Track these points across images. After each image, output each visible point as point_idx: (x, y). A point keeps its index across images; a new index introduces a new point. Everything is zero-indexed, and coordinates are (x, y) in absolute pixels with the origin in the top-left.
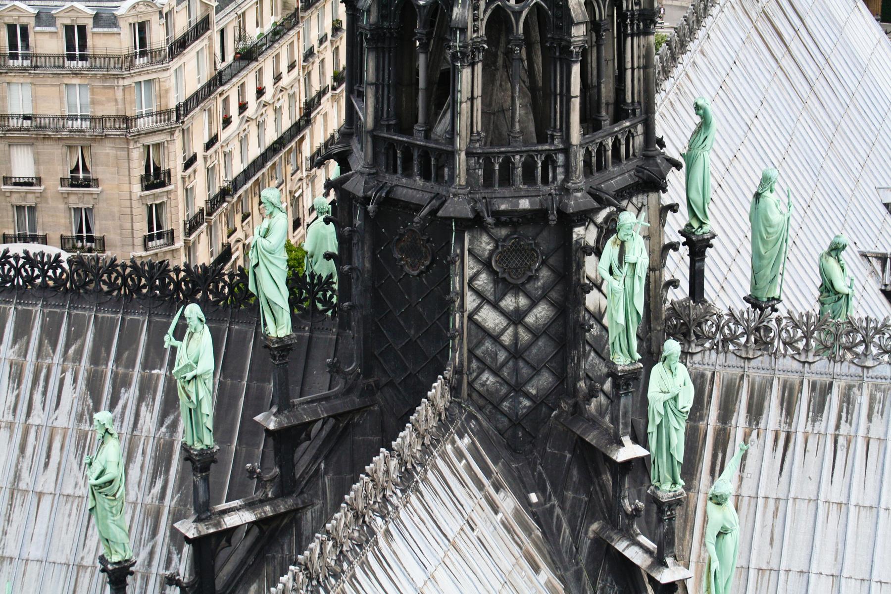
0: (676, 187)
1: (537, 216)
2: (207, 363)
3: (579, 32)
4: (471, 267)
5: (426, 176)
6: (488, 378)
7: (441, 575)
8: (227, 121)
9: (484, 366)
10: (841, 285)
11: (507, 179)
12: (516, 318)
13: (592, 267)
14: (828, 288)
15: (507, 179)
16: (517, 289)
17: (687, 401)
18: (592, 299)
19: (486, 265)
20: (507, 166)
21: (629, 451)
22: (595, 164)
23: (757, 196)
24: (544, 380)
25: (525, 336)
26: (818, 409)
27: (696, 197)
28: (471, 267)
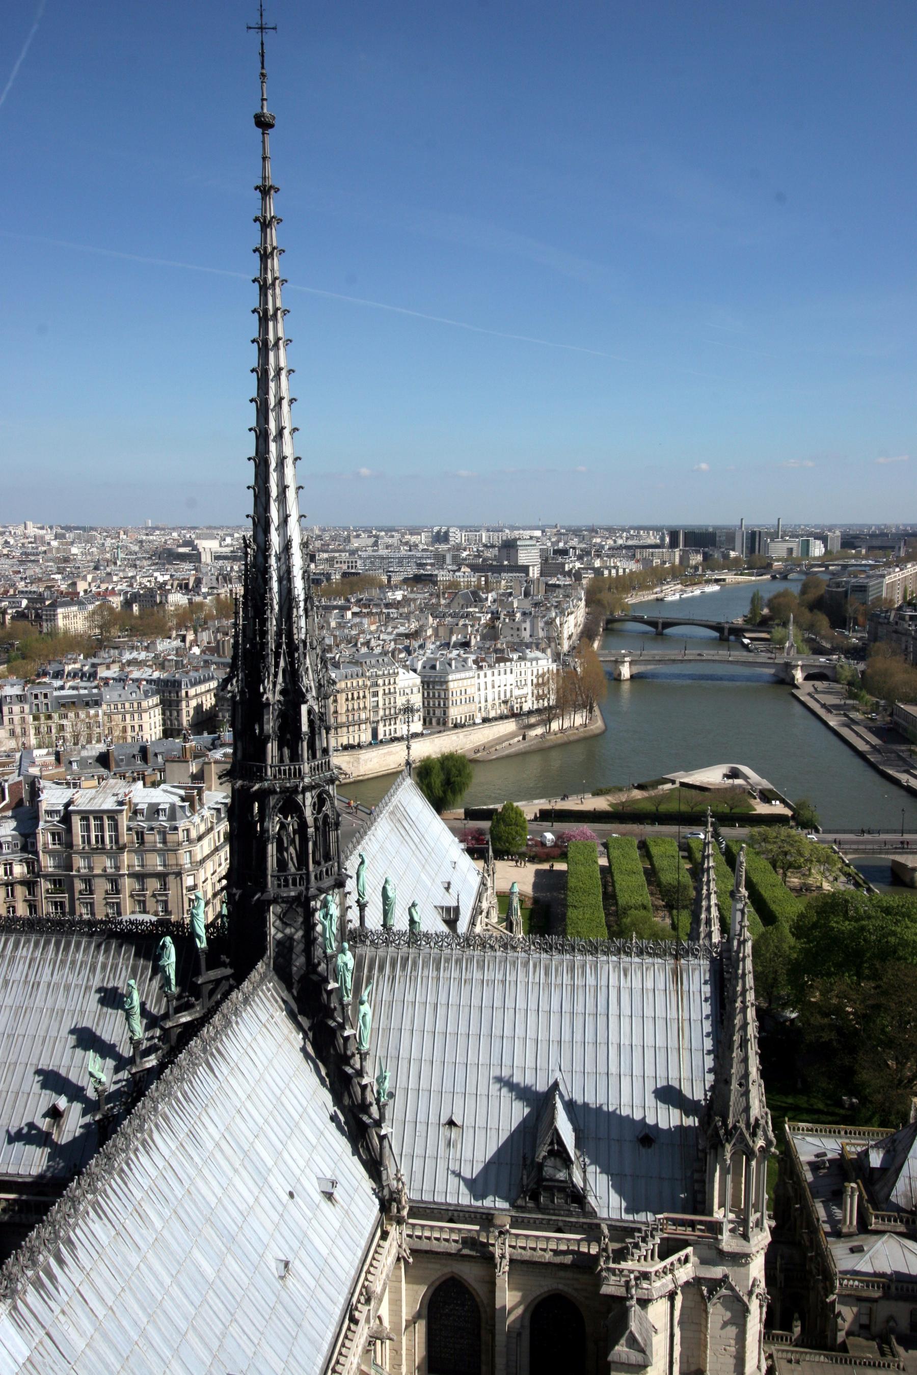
0: (350, 885)
1: (297, 898)
2: (173, 958)
3: (311, 830)
7: (259, 1037)
8: (220, 865)
10: (416, 918)
11: (286, 885)
13: (319, 915)
14: (412, 922)
15: (286, 885)
16: (290, 925)
17: (351, 964)
18: (319, 928)
20: (286, 880)
21: (332, 985)
22: (319, 878)
23: (384, 888)
26: (404, 967)
27: (361, 888)
28: (272, 918)
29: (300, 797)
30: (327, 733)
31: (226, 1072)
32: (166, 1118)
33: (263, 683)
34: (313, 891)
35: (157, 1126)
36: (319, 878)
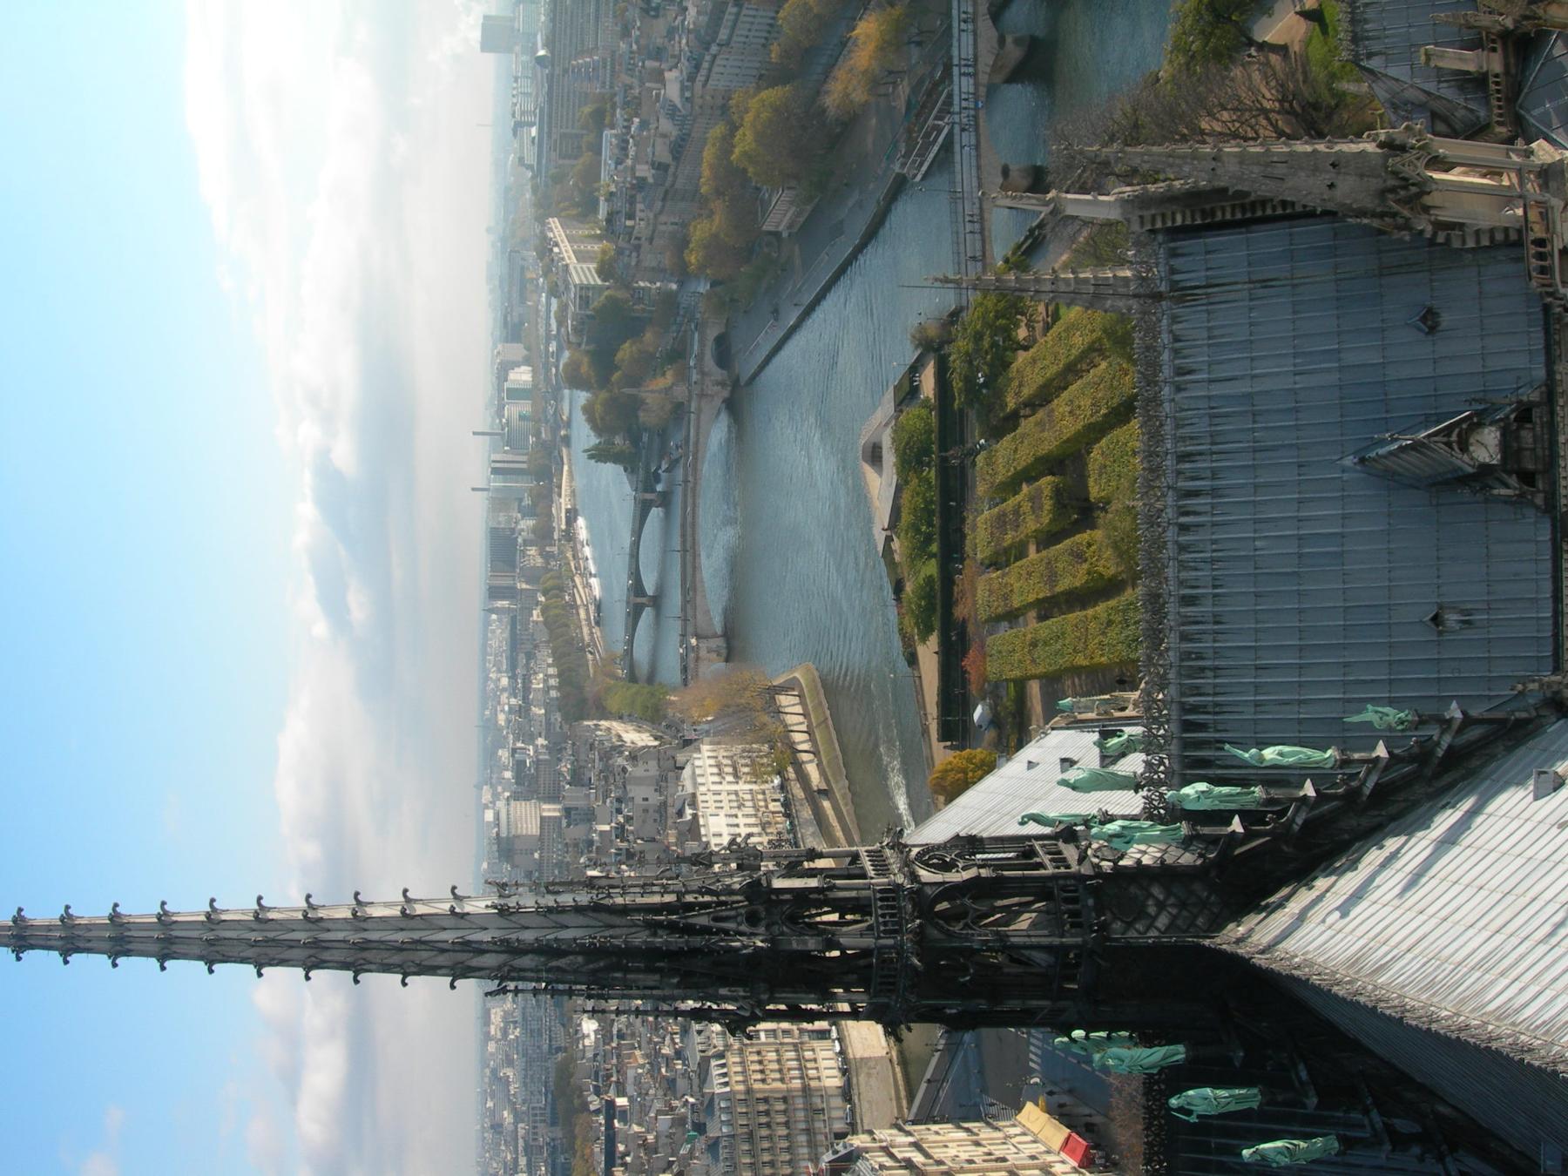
2: (1208, 1091)
3: (984, 873)
4: (1132, 934)
5: (1077, 965)
6: (1200, 921)
9: (1192, 924)
12: (1161, 906)
16: (1144, 906)
17: (1202, 786)
18: (1146, 860)
19: (1129, 925)
21: (1236, 825)
23: (1074, 788)
24: (1197, 887)
25: (1172, 900)
26: (1202, 727)
29: (929, 890)
30: (821, 856)
31: (1385, 949)
32: (1463, 1002)
33: (737, 950)
34: (1086, 870)
35: (1474, 1010)
36: (1060, 861)
